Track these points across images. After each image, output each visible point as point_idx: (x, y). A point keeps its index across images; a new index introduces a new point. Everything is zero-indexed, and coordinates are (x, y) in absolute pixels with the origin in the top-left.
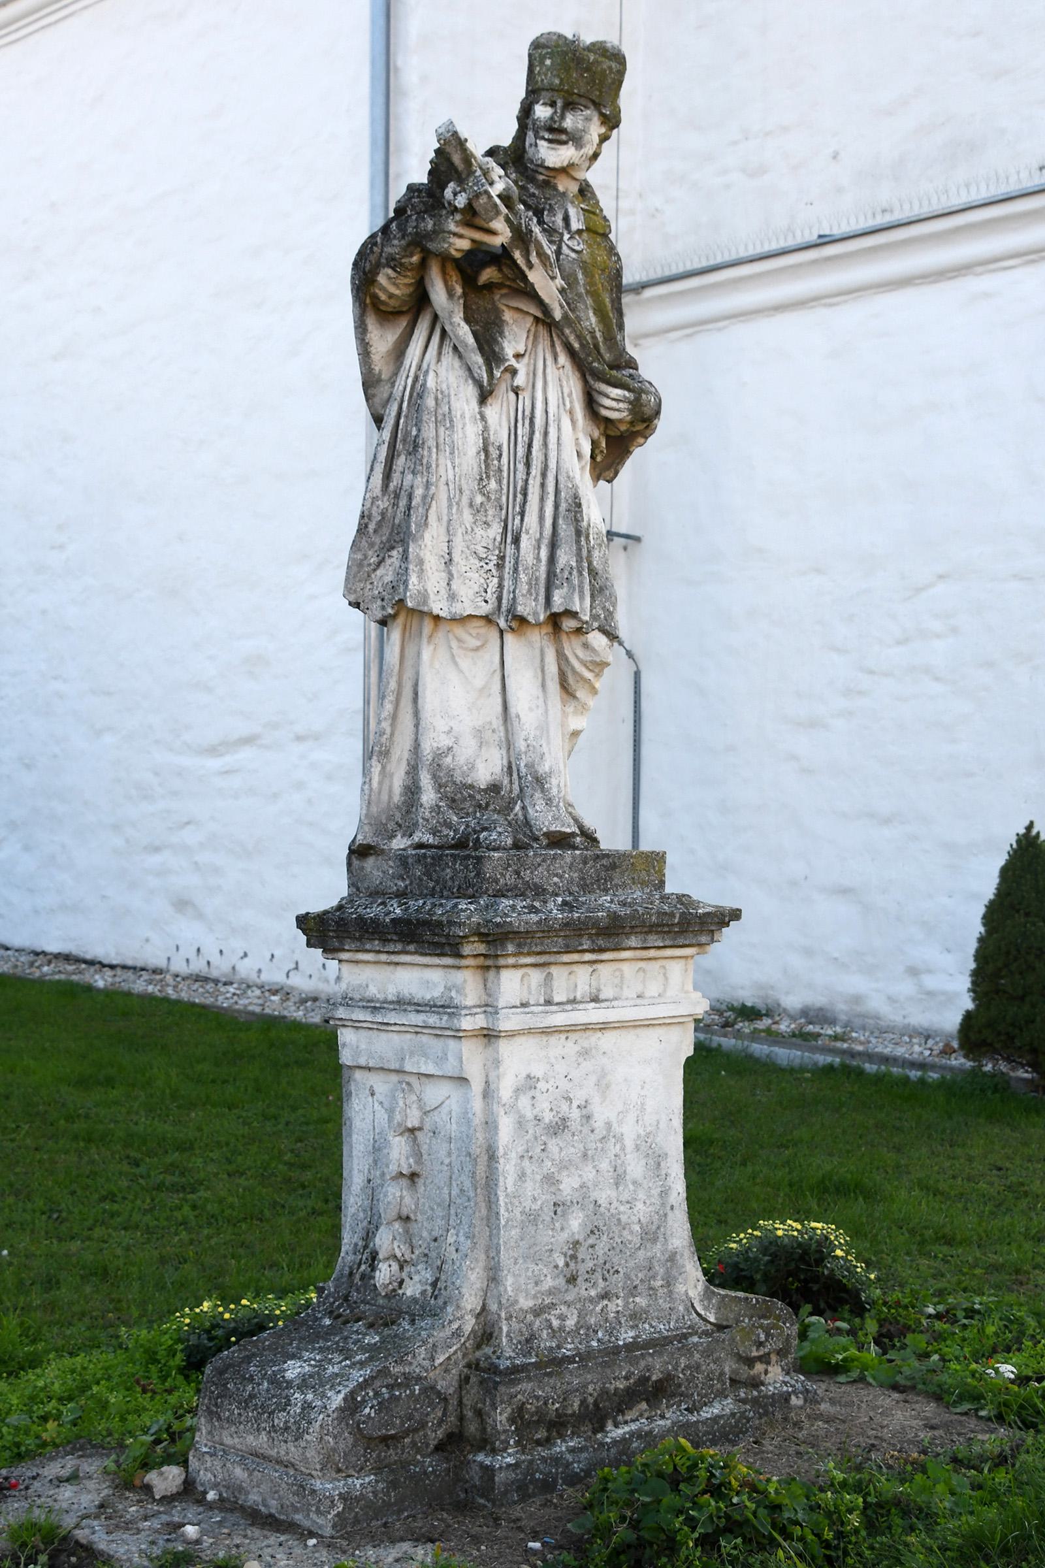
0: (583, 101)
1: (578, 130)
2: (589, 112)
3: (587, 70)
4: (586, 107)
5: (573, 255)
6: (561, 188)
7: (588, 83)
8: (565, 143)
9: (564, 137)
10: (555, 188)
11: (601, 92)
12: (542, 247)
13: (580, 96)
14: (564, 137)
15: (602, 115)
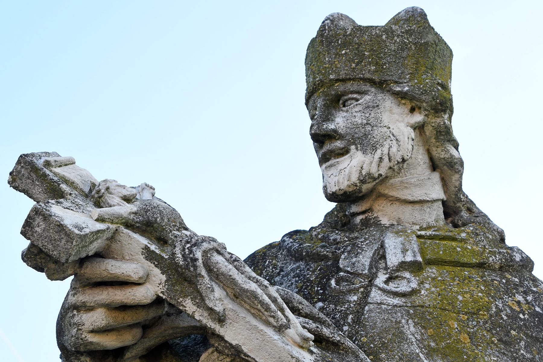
0: (349, 86)
1: (357, 126)
2: (367, 98)
3: (345, 45)
4: (362, 93)
5: (396, 301)
6: (385, 221)
7: (352, 61)
8: (345, 152)
9: (338, 144)
10: (377, 224)
11: (377, 64)
12: (233, 281)
13: (344, 81)
14: (338, 144)
15: (401, 96)
